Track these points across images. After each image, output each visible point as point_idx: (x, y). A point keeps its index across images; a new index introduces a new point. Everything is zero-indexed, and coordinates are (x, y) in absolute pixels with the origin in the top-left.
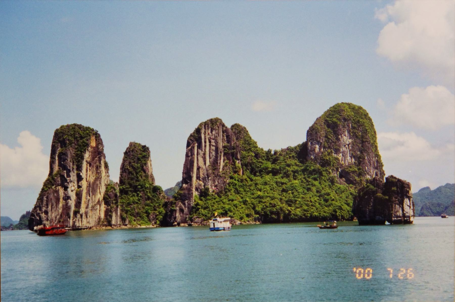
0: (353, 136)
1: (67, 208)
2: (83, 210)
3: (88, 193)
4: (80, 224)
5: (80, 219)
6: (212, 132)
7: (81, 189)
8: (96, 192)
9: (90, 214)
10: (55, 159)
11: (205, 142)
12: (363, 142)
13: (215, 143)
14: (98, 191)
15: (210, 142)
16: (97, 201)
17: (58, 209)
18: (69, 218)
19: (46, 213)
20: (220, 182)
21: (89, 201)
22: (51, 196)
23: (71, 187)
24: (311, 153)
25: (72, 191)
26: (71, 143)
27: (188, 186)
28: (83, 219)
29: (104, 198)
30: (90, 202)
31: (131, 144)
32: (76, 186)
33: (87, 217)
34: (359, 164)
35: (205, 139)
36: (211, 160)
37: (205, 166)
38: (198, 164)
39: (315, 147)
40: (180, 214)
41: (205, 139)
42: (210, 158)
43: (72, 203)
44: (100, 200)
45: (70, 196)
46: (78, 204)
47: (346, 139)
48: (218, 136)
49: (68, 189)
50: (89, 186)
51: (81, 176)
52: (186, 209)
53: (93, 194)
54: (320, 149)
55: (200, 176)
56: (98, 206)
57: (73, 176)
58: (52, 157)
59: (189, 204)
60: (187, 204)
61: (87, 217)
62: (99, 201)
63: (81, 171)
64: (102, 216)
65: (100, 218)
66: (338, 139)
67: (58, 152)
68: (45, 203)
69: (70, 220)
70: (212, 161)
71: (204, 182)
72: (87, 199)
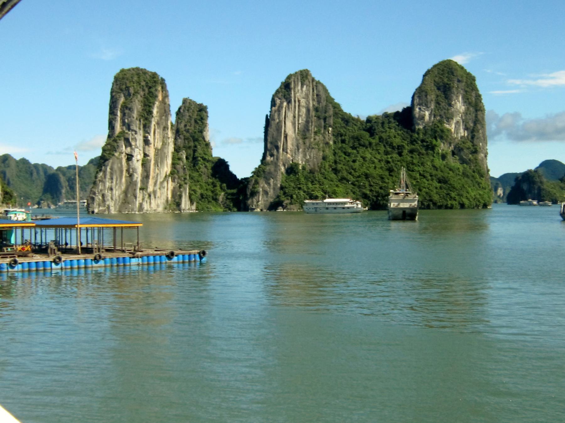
0: (466, 101)
1: (131, 183)
2: (150, 189)
3: (156, 164)
4: (149, 207)
5: (148, 201)
6: (302, 87)
7: (149, 158)
8: (164, 163)
9: (158, 194)
10: (116, 115)
11: (295, 101)
12: (476, 111)
13: (306, 104)
14: (166, 162)
16: (164, 176)
17: (121, 185)
18: (136, 197)
19: (111, 189)
20: (312, 156)
21: (157, 174)
22: (115, 167)
23: (137, 155)
24: (419, 122)
25: (138, 161)
26: (136, 93)
27: (274, 159)
28: (152, 201)
29: (172, 173)
31: (185, 101)
32: (142, 155)
33: (155, 197)
34: (473, 138)
35: (295, 97)
36: (300, 126)
37: (294, 134)
38: (285, 131)
39: (425, 115)
40: (263, 197)
43: (138, 176)
44: (168, 174)
45: (136, 167)
46: (145, 179)
48: (309, 93)
49: (133, 158)
50: (156, 155)
51: (149, 140)
52: (272, 191)
53: (161, 165)
54: (430, 118)
55: (288, 147)
58: (112, 112)
59: (275, 185)
60: (272, 184)
61: (155, 197)
62: (166, 177)
63: (149, 133)
64: (170, 196)
65: (167, 201)
66: (450, 105)
67: (120, 107)
68: (108, 176)
69: (136, 200)
70: (301, 127)
71: (292, 156)
72: (155, 173)
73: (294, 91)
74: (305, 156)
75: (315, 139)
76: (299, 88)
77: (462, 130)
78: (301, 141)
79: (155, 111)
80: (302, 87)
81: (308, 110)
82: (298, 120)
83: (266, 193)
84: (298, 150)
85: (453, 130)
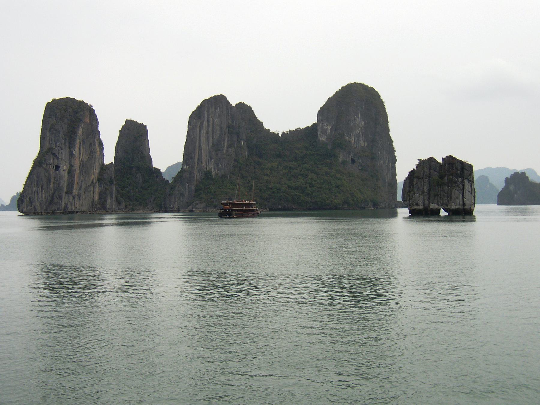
3: (81, 172)
11: (208, 121)
15: (213, 120)
29: (99, 180)
30: (83, 183)
41: (208, 118)
42: (213, 138)
47: (359, 121)
56: (92, 188)
57: (64, 154)
62: (92, 183)
64: (96, 198)
73: (208, 112)
74: (217, 165)
75: (227, 151)
76: (213, 110)
77: (362, 142)
78: (213, 153)
79: (80, 132)
80: (216, 109)
81: (221, 128)
82: (213, 137)
83: (182, 195)
84: (211, 160)
85: (353, 142)
